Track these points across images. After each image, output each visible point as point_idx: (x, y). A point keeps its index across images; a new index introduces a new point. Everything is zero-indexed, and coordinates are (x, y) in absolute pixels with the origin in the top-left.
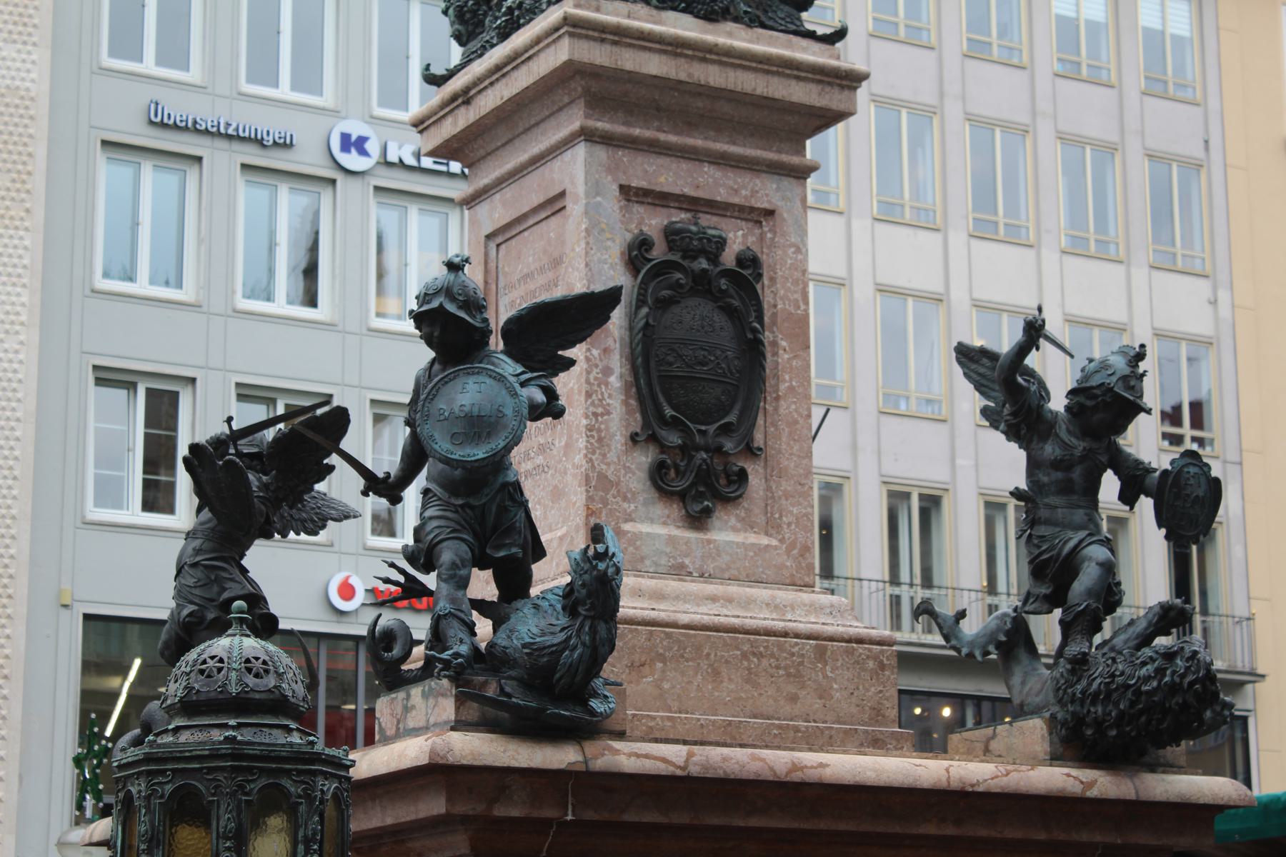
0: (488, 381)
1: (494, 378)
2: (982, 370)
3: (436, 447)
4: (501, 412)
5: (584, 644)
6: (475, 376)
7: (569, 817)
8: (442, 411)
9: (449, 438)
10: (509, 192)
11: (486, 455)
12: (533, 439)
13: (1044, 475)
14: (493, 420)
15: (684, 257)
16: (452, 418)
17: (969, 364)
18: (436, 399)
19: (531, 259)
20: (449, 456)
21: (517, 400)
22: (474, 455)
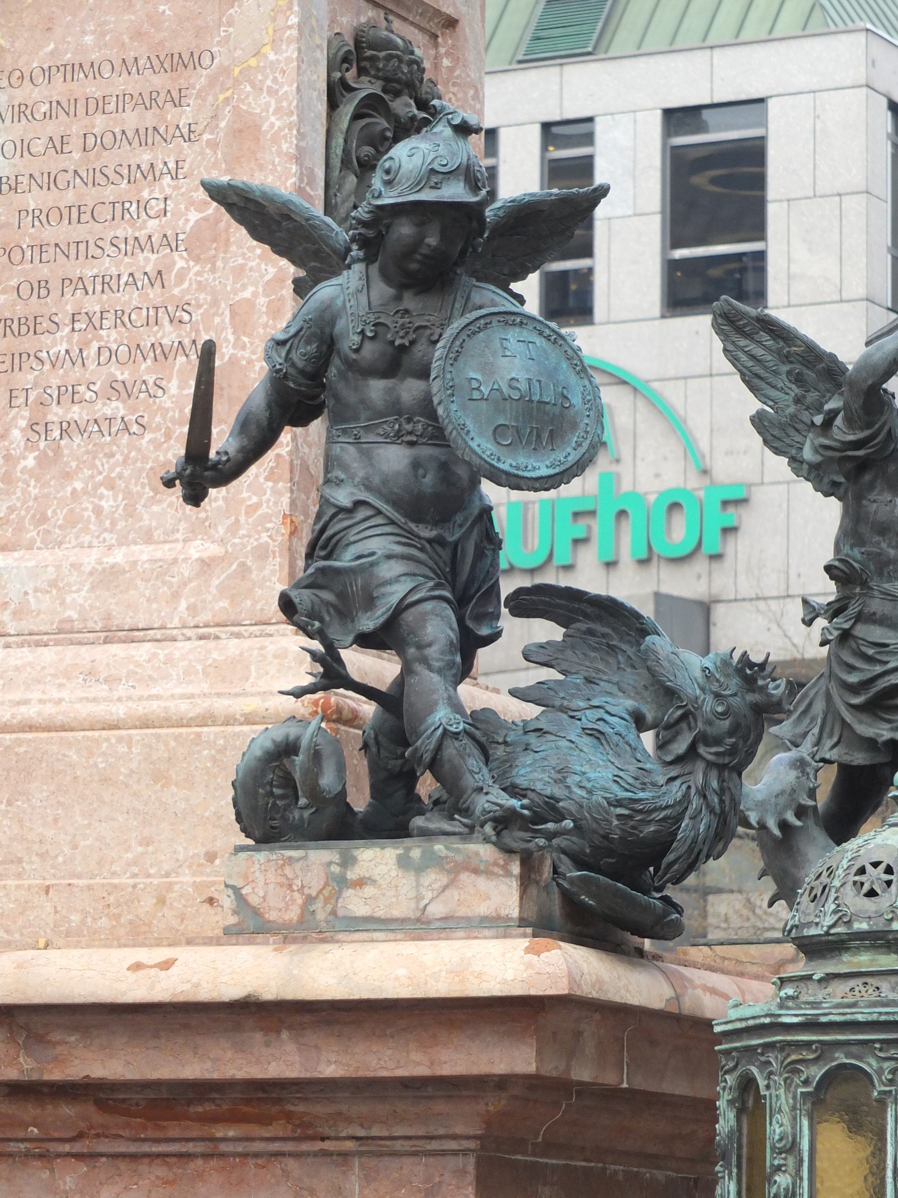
0: (539, 341)
1: (548, 338)
2: (759, 352)
3: (474, 445)
4: (566, 397)
5: (712, 811)
6: (517, 330)
7: (625, 1085)
8: (475, 384)
9: (491, 432)
11: (551, 472)
12: (92, 366)
13: (889, 546)
14: (557, 410)
15: (384, 90)
16: (499, 400)
17: (736, 337)
18: (461, 359)
19: (89, 39)
20: (494, 463)
21: (587, 383)
22: (534, 469)
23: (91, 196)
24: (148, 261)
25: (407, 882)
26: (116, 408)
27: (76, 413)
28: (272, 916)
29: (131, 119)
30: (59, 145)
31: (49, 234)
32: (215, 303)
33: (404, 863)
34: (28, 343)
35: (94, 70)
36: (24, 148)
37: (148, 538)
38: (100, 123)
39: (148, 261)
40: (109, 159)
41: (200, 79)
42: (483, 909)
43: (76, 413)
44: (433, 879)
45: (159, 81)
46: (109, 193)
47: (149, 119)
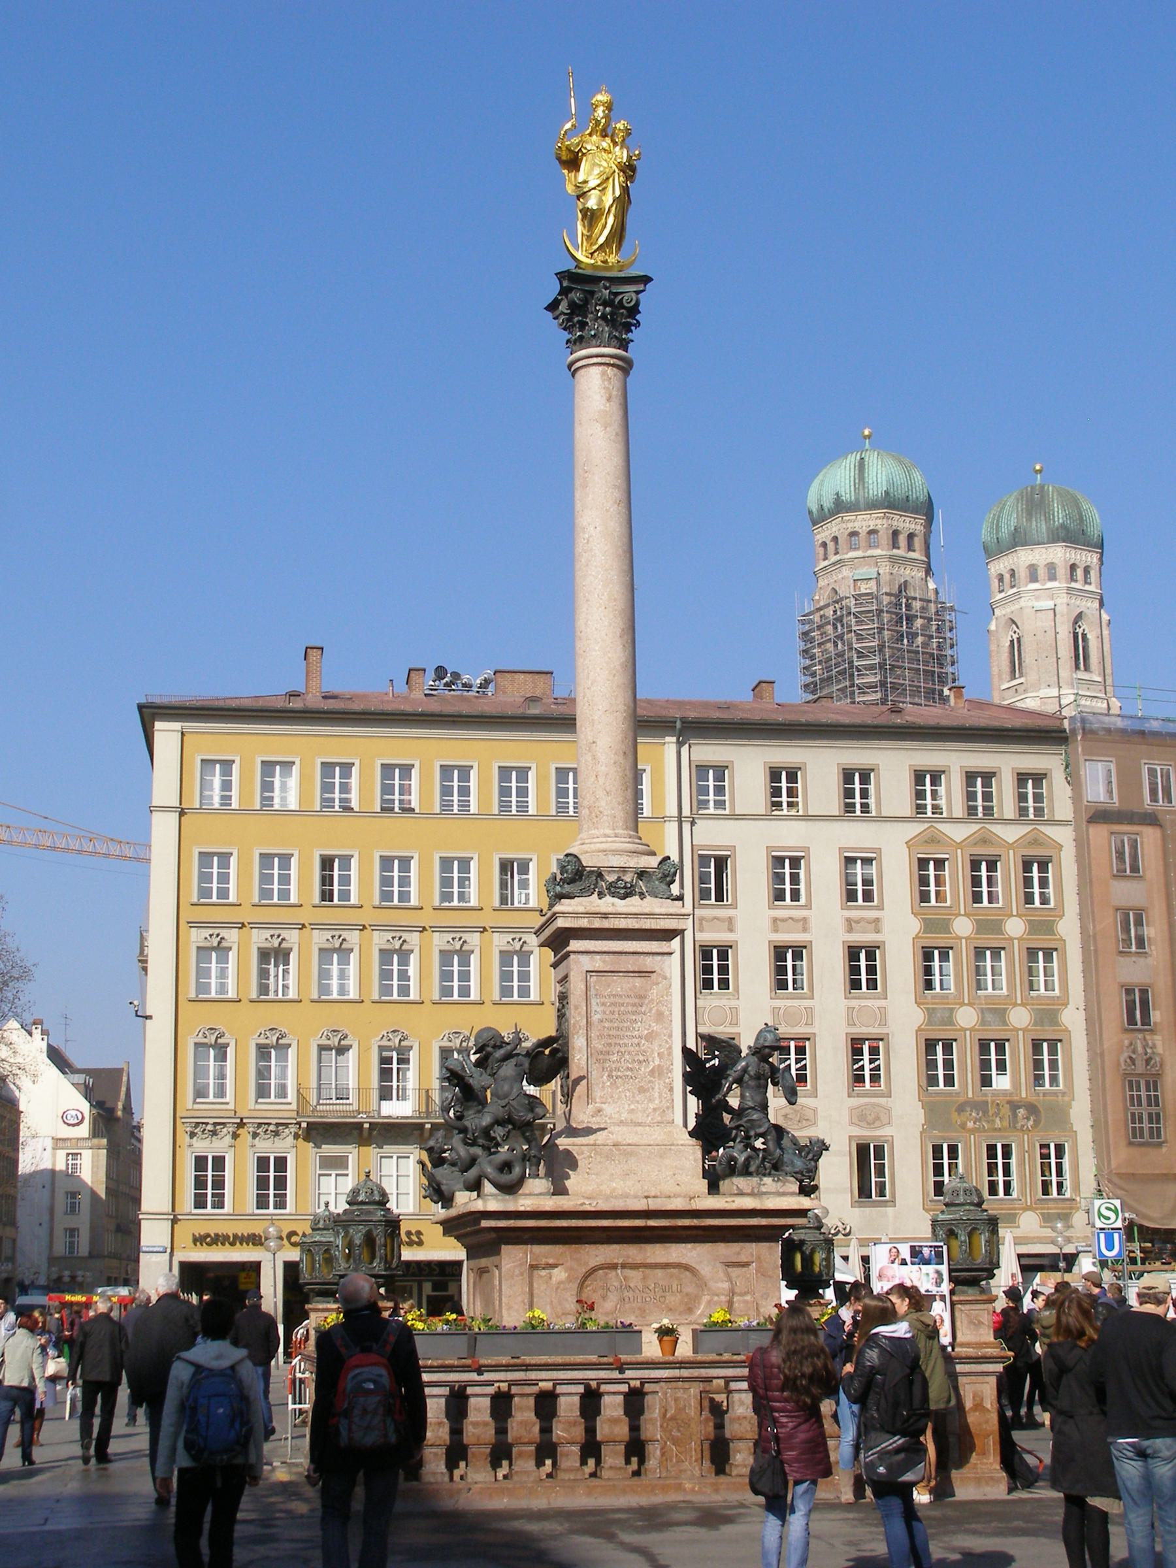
10: (606, 957)
23: (621, 1025)
24: (636, 1041)
25: (774, 1184)
26: (629, 1073)
27: (619, 1073)
28: (745, 1191)
29: (630, 1008)
30: (613, 1013)
31: (611, 1033)
32: (653, 1051)
33: (774, 1180)
34: (608, 1057)
35: (621, 996)
36: (604, 1013)
37: (638, 1102)
38: (622, 1008)
39: (636, 1041)
40: (625, 1017)
41: (647, 1001)
42: (791, 1190)
43: (619, 1073)
44: (780, 1184)
45: (637, 1001)
46: (625, 1025)
47: (635, 1009)
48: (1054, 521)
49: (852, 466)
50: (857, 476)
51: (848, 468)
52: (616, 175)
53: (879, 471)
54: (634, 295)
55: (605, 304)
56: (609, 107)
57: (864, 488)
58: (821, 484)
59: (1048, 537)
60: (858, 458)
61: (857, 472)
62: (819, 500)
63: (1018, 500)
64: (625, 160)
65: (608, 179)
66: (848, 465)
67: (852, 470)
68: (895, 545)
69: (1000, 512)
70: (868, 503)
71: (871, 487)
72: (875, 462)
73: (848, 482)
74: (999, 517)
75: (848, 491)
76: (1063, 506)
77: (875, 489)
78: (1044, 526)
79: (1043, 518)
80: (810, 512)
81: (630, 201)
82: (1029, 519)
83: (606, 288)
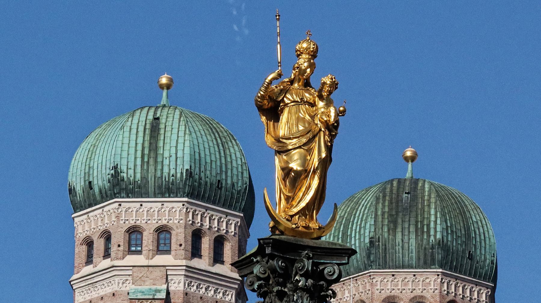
48: (429, 236)
49: (141, 129)
50: (147, 144)
51: (134, 131)
52: (322, 133)
53: (181, 140)
54: (336, 267)
55: (306, 275)
56: (314, 55)
57: (156, 162)
58: (92, 152)
59: (419, 259)
60: (151, 117)
61: (147, 138)
62: (88, 174)
63: (378, 199)
64: (332, 119)
65: (314, 137)
66: (134, 127)
67: (141, 134)
68: (196, 252)
69: (350, 214)
70: (160, 187)
71: (166, 162)
72: (176, 125)
73: (132, 151)
74: (348, 220)
75: (131, 165)
76: (443, 215)
77: (173, 166)
78: (413, 241)
79: (412, 229)
80: (72, 191)
81: (331, 160)
82: (393, 230)
83: (309, 258)
